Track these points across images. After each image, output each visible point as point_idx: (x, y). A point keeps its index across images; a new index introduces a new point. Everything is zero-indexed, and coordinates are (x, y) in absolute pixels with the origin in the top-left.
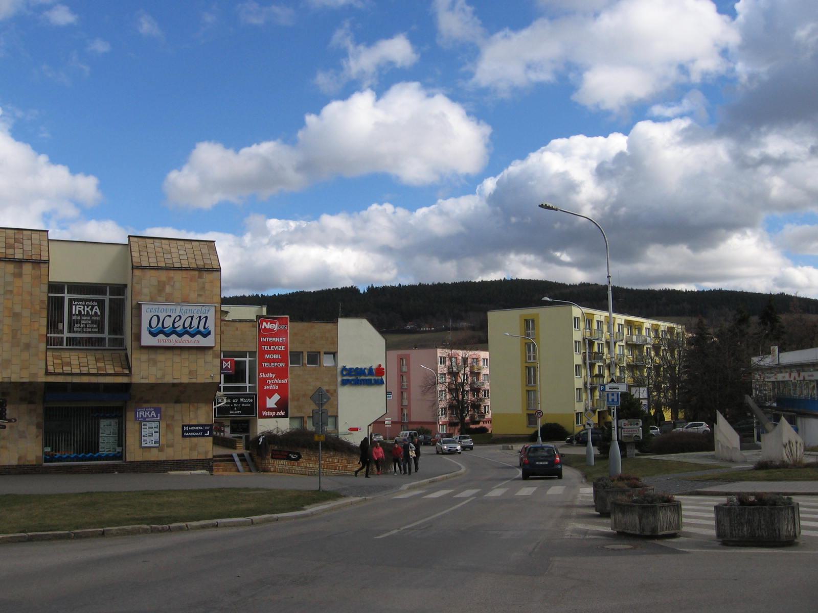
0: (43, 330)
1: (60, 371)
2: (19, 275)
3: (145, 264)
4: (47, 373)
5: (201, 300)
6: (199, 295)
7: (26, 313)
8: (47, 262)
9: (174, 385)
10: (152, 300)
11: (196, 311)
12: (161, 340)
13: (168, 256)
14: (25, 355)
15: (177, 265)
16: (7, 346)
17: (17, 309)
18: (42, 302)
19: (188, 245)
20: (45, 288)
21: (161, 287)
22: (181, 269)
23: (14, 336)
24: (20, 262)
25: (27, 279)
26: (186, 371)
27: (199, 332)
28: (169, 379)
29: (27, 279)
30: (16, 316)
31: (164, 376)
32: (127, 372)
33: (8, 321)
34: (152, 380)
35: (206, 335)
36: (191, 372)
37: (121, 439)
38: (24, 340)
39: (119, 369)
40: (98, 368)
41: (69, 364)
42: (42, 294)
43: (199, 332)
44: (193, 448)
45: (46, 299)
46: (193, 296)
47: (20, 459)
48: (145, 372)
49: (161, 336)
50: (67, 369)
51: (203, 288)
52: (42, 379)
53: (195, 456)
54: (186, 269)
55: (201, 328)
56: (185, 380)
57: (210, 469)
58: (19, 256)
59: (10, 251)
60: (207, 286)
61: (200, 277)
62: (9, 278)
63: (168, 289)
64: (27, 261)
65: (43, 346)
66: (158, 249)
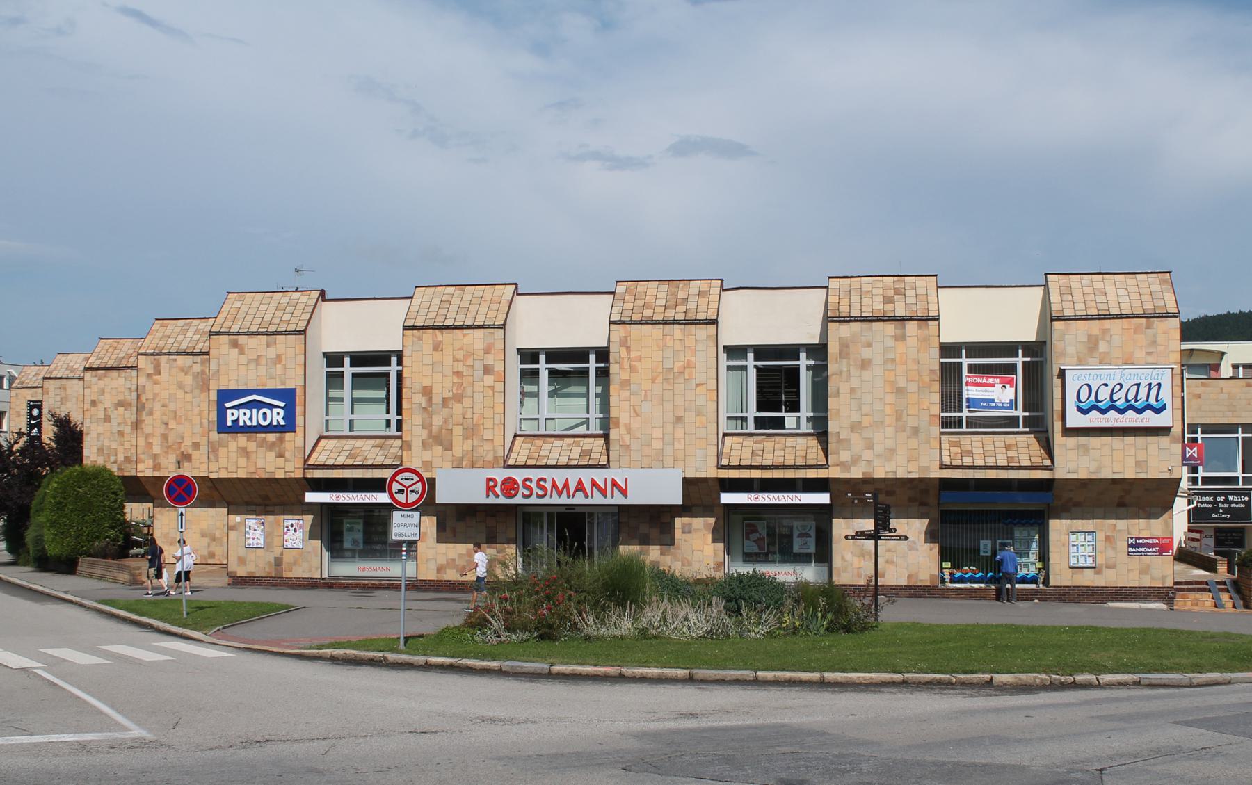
0: (936, 409)
1: (958, 463)
2: (901, 338)
3: (1068, 312)
4: (943, 467)
5: (1150, 359)
6: (1149, 353)
7: (912, 387)
8: (936, 319)
9: (1114, 481)
10: (1081, 363)
11: (1146, 377)
12: (1094, 420)
13: (1101, 299)
14: (913, 443)
15: (1115, 311)
16: (890, 431)
17: (902, 383)
18: (932, 371)
19: (1130, 280)
20: (936, 352)
21: (1092, 344)
22: (1120, 317)
23: (899, 419)
24: (903, 320)
25: (912, 342)
26: (1131, 462)
27: (1149, 407)
28: (1107, 474)
29: (912, 342)
30: (900, 391)
31: (1099, 469)
32: (1048, 462)
33: (890, 399)
34: (1083, 475)
35: (1158, 411)
36: (1138, 464)
37: (1044, 557)
38: (912, 422)
39: (1037, 460)
40: (1010, 459)
41: (970, 453)
42: (934, 360)
43: (1149, 407)
44: (1145, 571)
45: (937, 368)
46: (1139, 354)
47: (909, 577)
48: (1075, 462)
49: (1094, 413)
50: (967, 461)
51: (1154, 342)
52: (936, 473)
53: (1147, 582)
54: (1128, 317)
55: (1152, 401)
56: (1130, 474)
57: (1170, 601)
58: (900, 312)
59: (889, 307)
60: (1160, 339)
61: (1148, 327)
62: (890, 343)
63: (1103, 347)
64: (911, 320)
65: (936, 430)
66: (1087, 290)
